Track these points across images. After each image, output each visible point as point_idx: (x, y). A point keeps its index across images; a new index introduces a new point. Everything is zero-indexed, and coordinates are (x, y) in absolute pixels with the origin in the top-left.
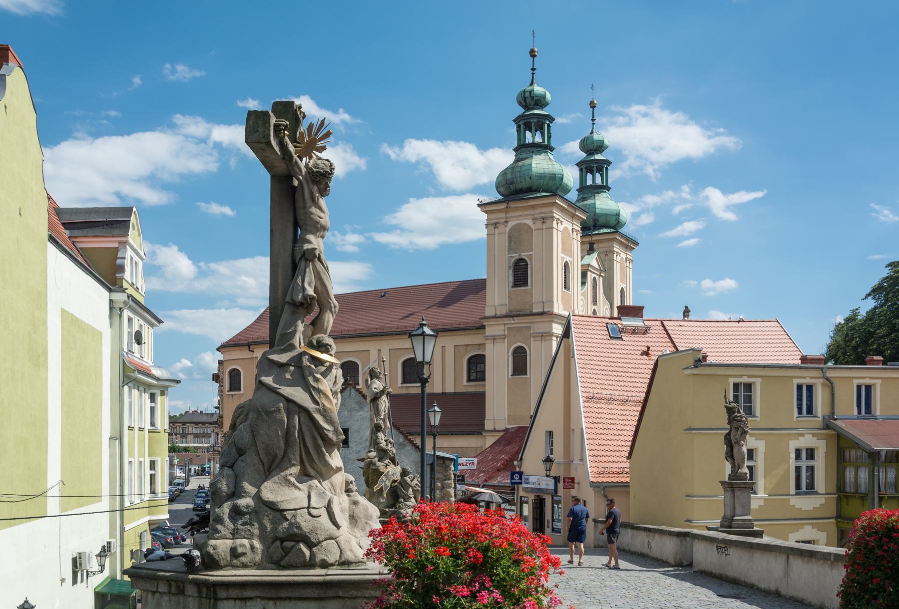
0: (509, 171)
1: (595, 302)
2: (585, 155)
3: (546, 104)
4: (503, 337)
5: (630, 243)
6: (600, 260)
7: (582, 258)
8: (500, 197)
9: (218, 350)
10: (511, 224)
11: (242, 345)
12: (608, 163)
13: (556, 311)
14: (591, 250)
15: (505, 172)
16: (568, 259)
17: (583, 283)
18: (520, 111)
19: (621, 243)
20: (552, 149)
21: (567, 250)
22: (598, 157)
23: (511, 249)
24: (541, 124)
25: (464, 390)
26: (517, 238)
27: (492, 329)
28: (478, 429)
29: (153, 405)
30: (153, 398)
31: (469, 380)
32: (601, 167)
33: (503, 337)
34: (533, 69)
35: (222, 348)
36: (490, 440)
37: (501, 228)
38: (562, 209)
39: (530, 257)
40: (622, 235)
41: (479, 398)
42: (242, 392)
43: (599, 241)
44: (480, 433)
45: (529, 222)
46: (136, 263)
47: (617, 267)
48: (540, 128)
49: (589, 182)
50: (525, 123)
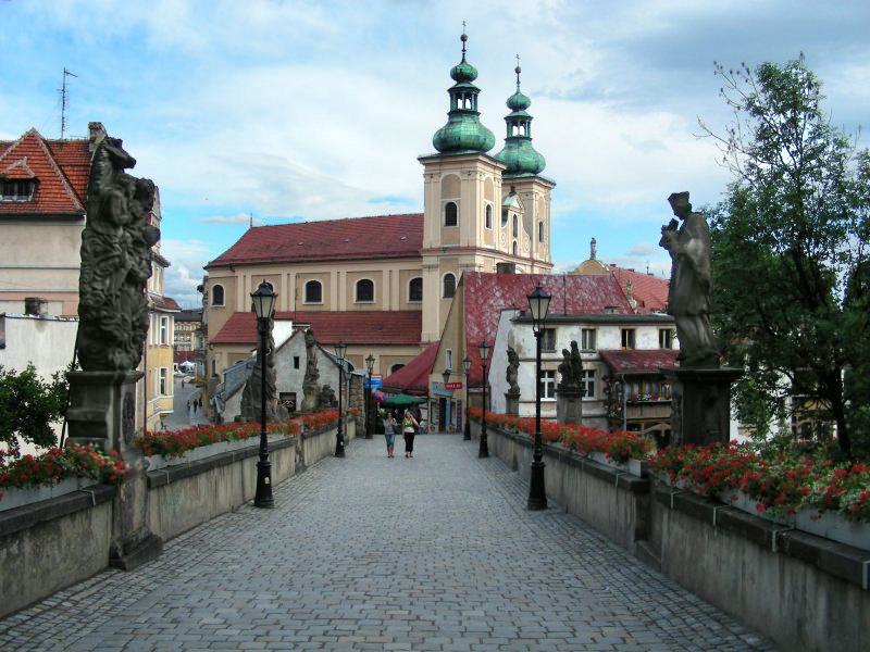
0: (443, 132)
1: (515, 235)
2: (511, 111)
3: (474, 79)
4: (437, 267)
5: (549, 184)
6: (521, 201)
7: (503, 200)
8: (437, 152)
10: (443, 176)
11: (225, 266)
12: (530, 118)
13: (478, 245)
14: (513, 193)
15: (439, 133)
16: (489, 202)
17: (504, 220)
18: (453, 83)
19: (540, 185)
20: (478, 114)
21: (489, 195)
22: (521, 113)
23: (444, 195)
24: (472, 93)
25: (406, 308)
26: (449, 186)
27: (428, 260)
28: (415, 341)
31: (412, 298)
32: (525, 121)
33: (437, 267)
34: (464, 50)
35: (210, 267)
36: (424, 349)
37: (435, 177)
38: (485, 163)
39: (459, 202)
40: (540, 179)
41: (415, 318)
43: (520, 184)
44: (418, 345)
45: (458, 174)
47: (535, 204)
48: (468, 96)
49: (515, 133)
50: (455, 93)
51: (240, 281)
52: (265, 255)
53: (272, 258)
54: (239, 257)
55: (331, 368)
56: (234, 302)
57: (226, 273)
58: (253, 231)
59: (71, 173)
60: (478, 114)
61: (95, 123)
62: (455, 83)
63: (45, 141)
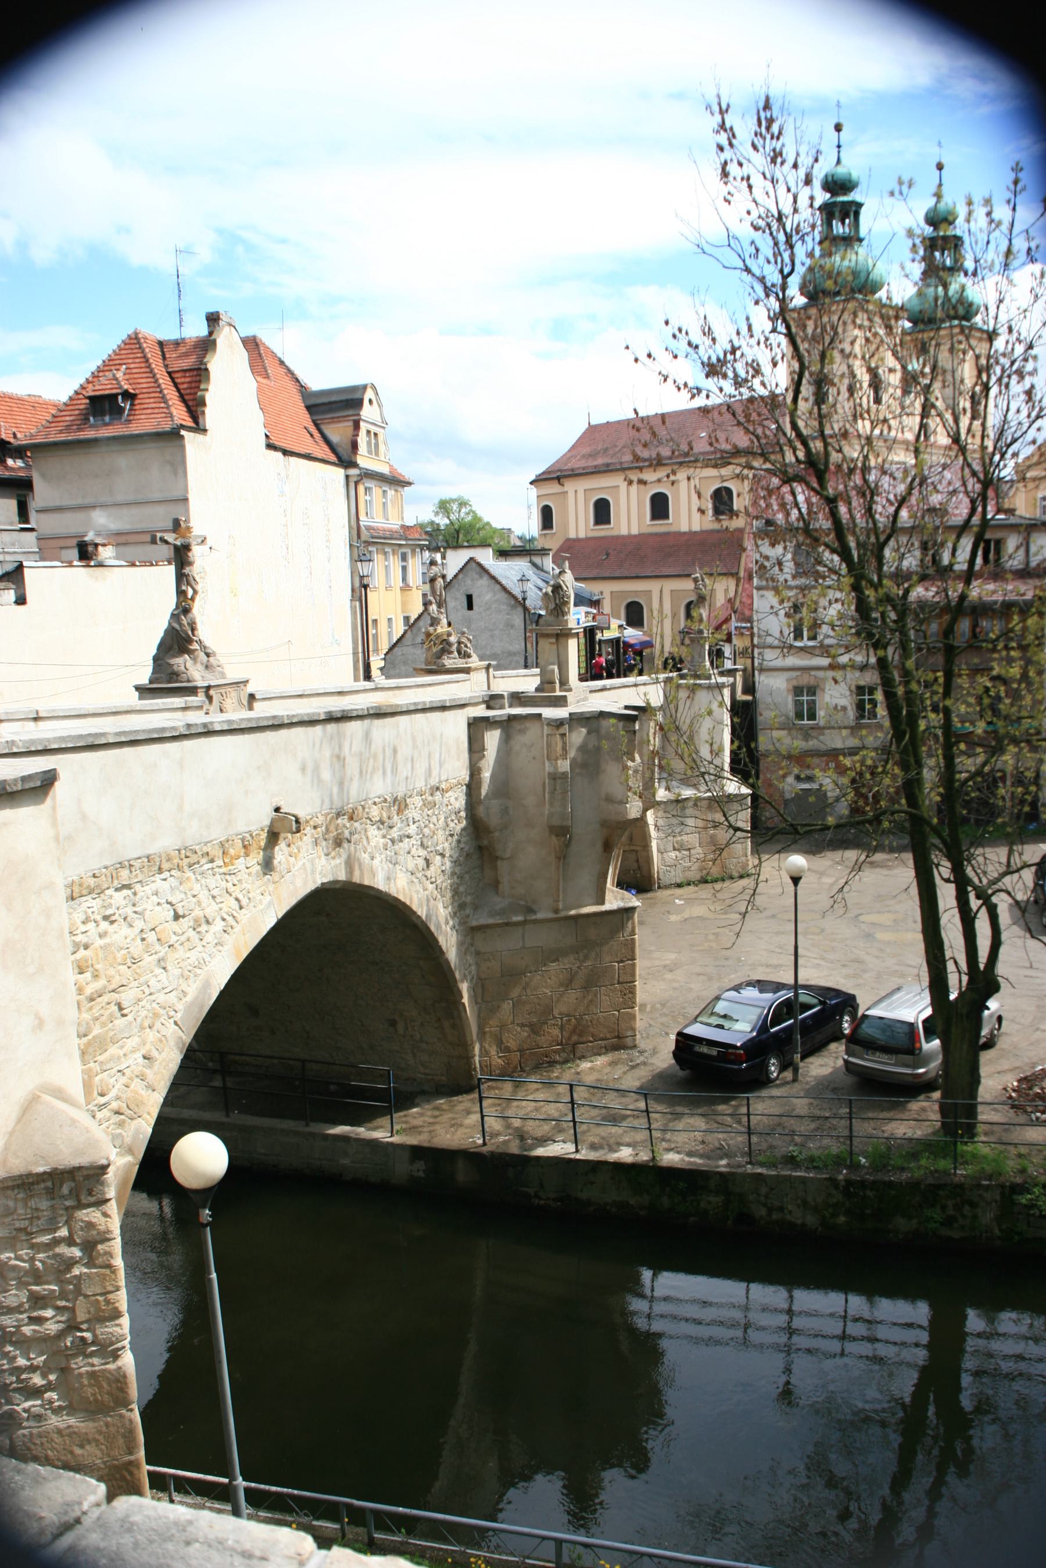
9: (531, 483)
20: (861, 240)
29: (404, 564)
30: (404, 558)
42: (554, 531)
46: (376, 434)
51: (571, 495)
52: (600, 461)
53: (608, 465)
54: (569, 466)
55: (513, 607)
56: (565, 526)
57: (553, 488)
58: (593, 431)
59: (183, 380)
60: (861, 240)
61: (212, 314)
62: (828, 195)
63: (161, 344)
